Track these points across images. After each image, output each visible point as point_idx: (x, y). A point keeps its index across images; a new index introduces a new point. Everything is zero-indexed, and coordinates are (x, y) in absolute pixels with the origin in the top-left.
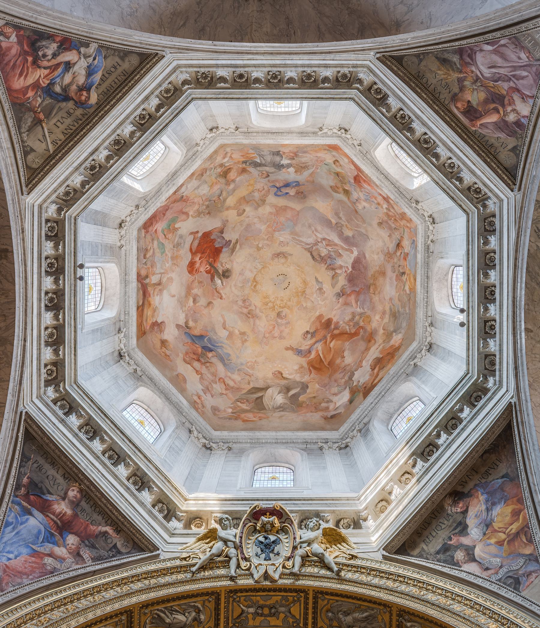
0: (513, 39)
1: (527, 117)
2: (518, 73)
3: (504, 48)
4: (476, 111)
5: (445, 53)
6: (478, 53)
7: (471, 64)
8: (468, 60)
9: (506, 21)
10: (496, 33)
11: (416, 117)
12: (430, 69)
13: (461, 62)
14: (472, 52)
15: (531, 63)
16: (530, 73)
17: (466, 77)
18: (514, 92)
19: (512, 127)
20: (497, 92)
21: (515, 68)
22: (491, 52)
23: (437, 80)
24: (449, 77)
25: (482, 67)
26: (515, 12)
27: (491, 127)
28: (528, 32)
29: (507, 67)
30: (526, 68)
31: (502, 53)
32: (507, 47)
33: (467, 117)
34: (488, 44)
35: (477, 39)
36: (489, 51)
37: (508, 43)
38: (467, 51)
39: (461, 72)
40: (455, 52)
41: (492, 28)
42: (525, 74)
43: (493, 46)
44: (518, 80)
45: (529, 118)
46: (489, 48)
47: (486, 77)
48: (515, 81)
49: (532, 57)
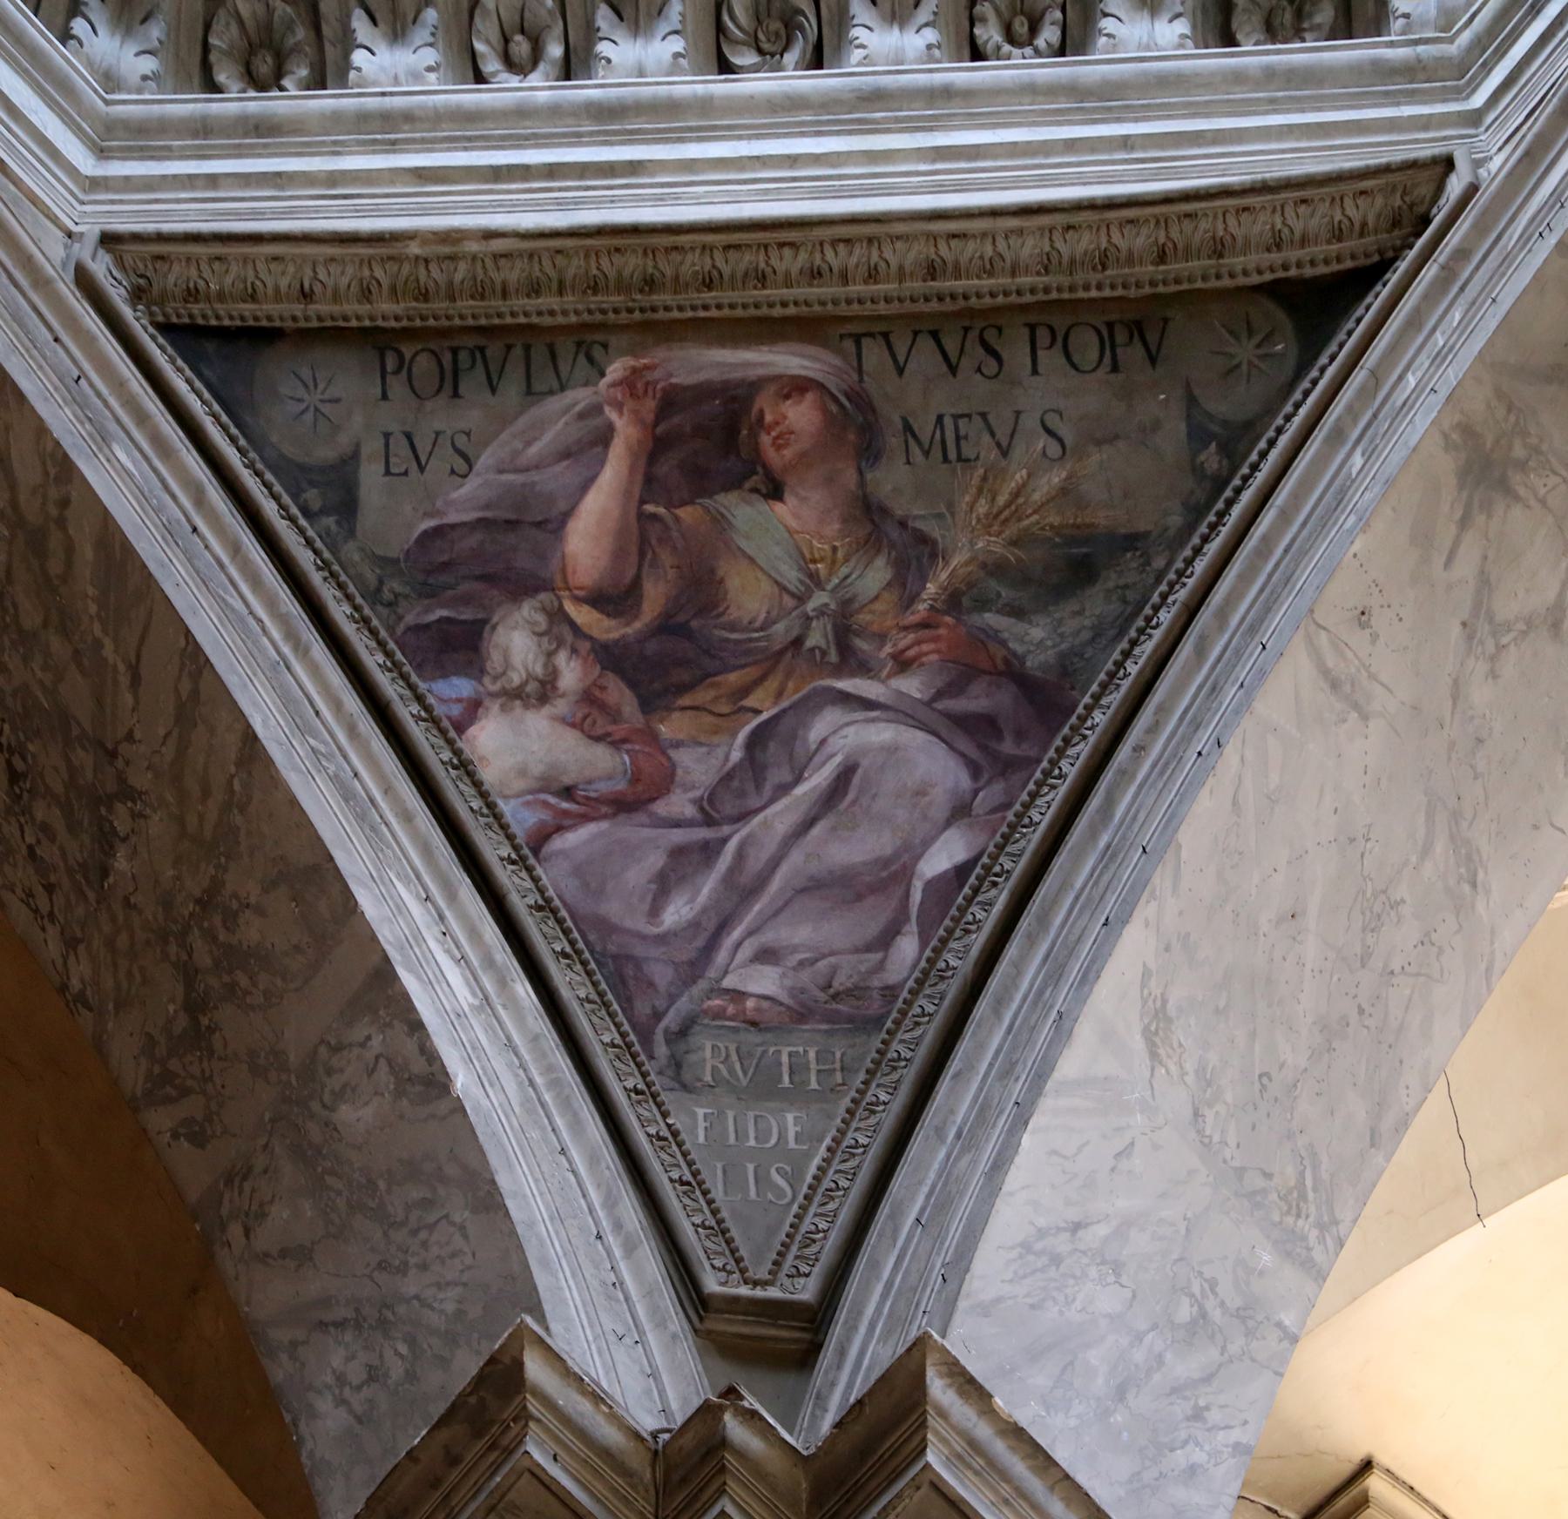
0: (875, 1006)
1: (461, 728)
2: (708, 886)
3: (873, 928)
4: (701, 483)
5: (1114, 608)
6: (965, 782)
7: (939, 695)
8: (976, 701)
9: (981, 1047)
10: (975, 952)
11: (947, 93)
12: (1113, 439)
13: (1000, 653)
14: (995, 756)
15: (702, 985)
16: (662, 939)
17: (910, 601)
18: (635, 779)
19: (466, 600)
20: (702, 696)
21: (740, 890)
22: (913, 851)
23: (1030, 422)
24: (982, 508)
25: (882, 733)
26: (983, 1113)
27: (555, 478)
28: (846, 1102)
29: (774, 863)
30: (700, 942)
31: (859, 897)
32: (868, 948)
33: (704, 392)
34: (961, 872)
35: (1031, 841)
36: (927, 843)
37: (880, 967)
38: (1020, 735)
39: (953, 601)
40: (1070, 670)
41: (1012, 951)
42: (677, 912)
43: (929, 884)
44: (678, 853)
45: (453, 729)
46: (940, 860)
47: (819, 708)
48: (678, 836)
49: (719, 1014)
